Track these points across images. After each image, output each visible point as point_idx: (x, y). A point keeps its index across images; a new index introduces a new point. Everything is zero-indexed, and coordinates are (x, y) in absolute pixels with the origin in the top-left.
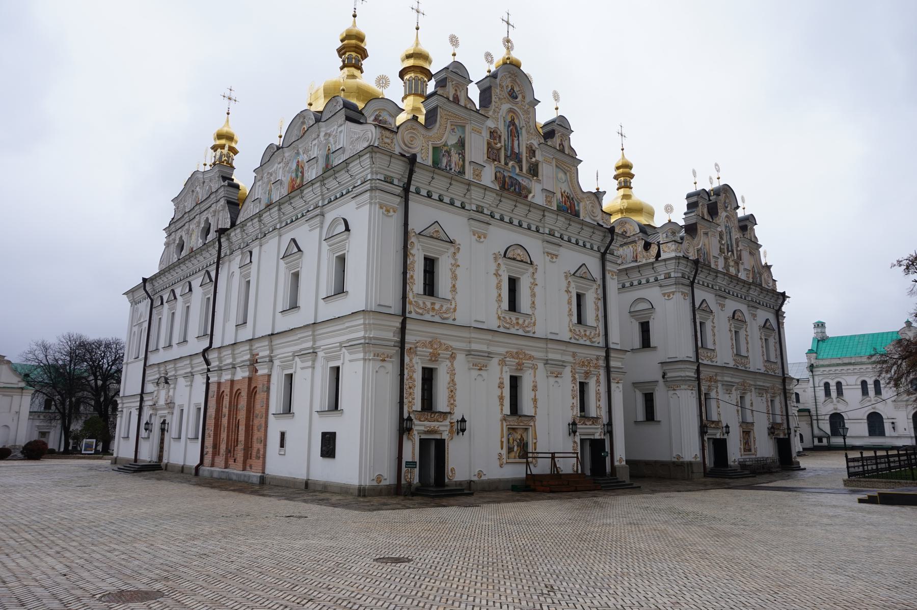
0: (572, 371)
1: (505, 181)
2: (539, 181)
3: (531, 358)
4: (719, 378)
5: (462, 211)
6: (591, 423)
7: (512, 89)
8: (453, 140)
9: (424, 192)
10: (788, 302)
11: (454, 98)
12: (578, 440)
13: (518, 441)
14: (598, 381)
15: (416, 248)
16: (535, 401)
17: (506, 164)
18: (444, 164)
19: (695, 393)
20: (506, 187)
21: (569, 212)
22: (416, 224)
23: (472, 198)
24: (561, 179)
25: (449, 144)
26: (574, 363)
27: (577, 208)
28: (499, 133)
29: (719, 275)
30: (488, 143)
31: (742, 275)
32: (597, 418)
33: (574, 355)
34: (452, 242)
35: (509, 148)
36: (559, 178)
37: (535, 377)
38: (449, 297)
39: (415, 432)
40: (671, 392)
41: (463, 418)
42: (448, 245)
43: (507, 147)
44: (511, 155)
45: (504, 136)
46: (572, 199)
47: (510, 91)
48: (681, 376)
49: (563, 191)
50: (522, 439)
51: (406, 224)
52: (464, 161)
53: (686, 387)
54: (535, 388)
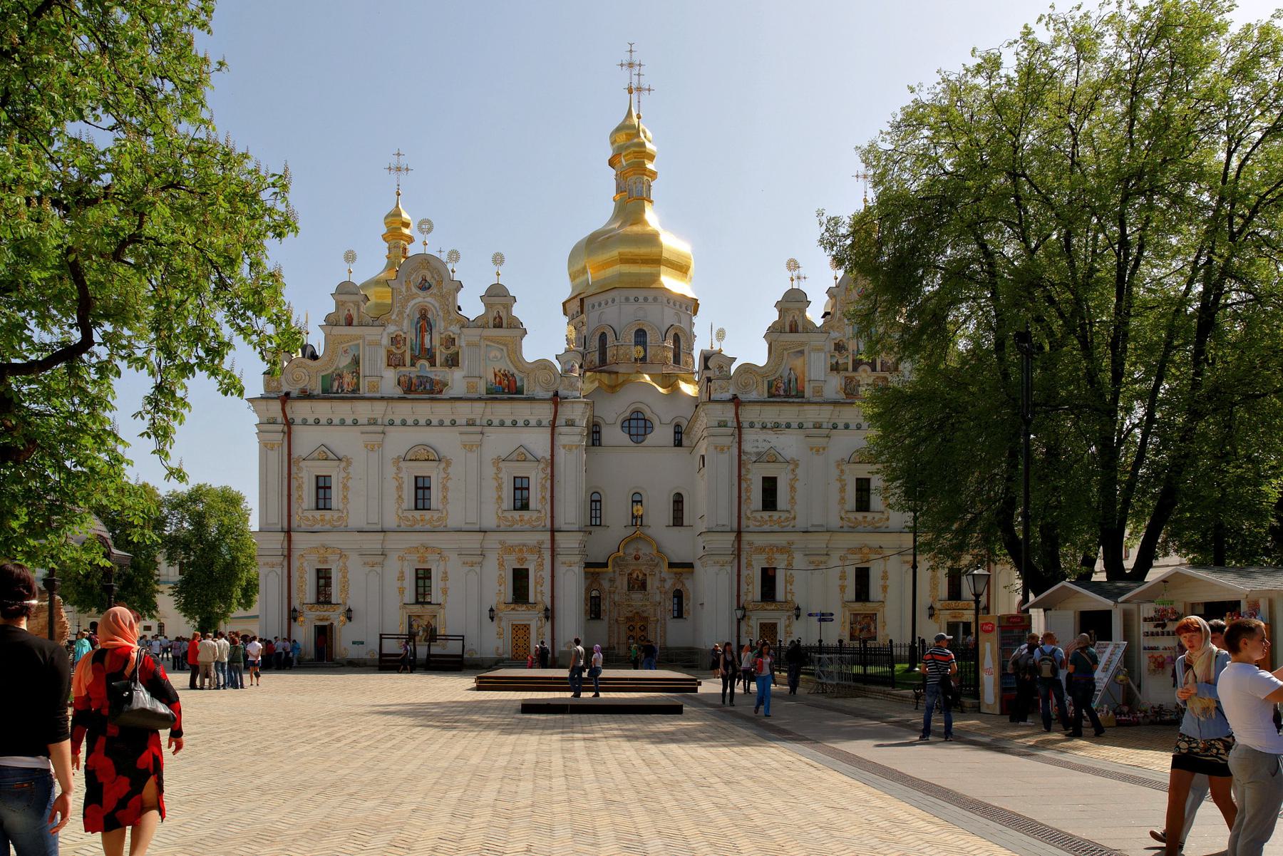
5: (355, 428)
6: (524, 607)
7: (424, 280)
8: (345, 361)
11: (346, 319)
12: (506, 626)
16: (445, 592)
18: (335, 389)
19: (730, 570)
22: (301, 449)
24: (496, 357)
27: (519, 384)
28: (403, 336)
30: (390, 354)
33: (502, 543)
38: (341, 508)
45: (411, 336)
46: (513, 375)
50: (429, 625)
52: (358, 378)
54: (445, 578)
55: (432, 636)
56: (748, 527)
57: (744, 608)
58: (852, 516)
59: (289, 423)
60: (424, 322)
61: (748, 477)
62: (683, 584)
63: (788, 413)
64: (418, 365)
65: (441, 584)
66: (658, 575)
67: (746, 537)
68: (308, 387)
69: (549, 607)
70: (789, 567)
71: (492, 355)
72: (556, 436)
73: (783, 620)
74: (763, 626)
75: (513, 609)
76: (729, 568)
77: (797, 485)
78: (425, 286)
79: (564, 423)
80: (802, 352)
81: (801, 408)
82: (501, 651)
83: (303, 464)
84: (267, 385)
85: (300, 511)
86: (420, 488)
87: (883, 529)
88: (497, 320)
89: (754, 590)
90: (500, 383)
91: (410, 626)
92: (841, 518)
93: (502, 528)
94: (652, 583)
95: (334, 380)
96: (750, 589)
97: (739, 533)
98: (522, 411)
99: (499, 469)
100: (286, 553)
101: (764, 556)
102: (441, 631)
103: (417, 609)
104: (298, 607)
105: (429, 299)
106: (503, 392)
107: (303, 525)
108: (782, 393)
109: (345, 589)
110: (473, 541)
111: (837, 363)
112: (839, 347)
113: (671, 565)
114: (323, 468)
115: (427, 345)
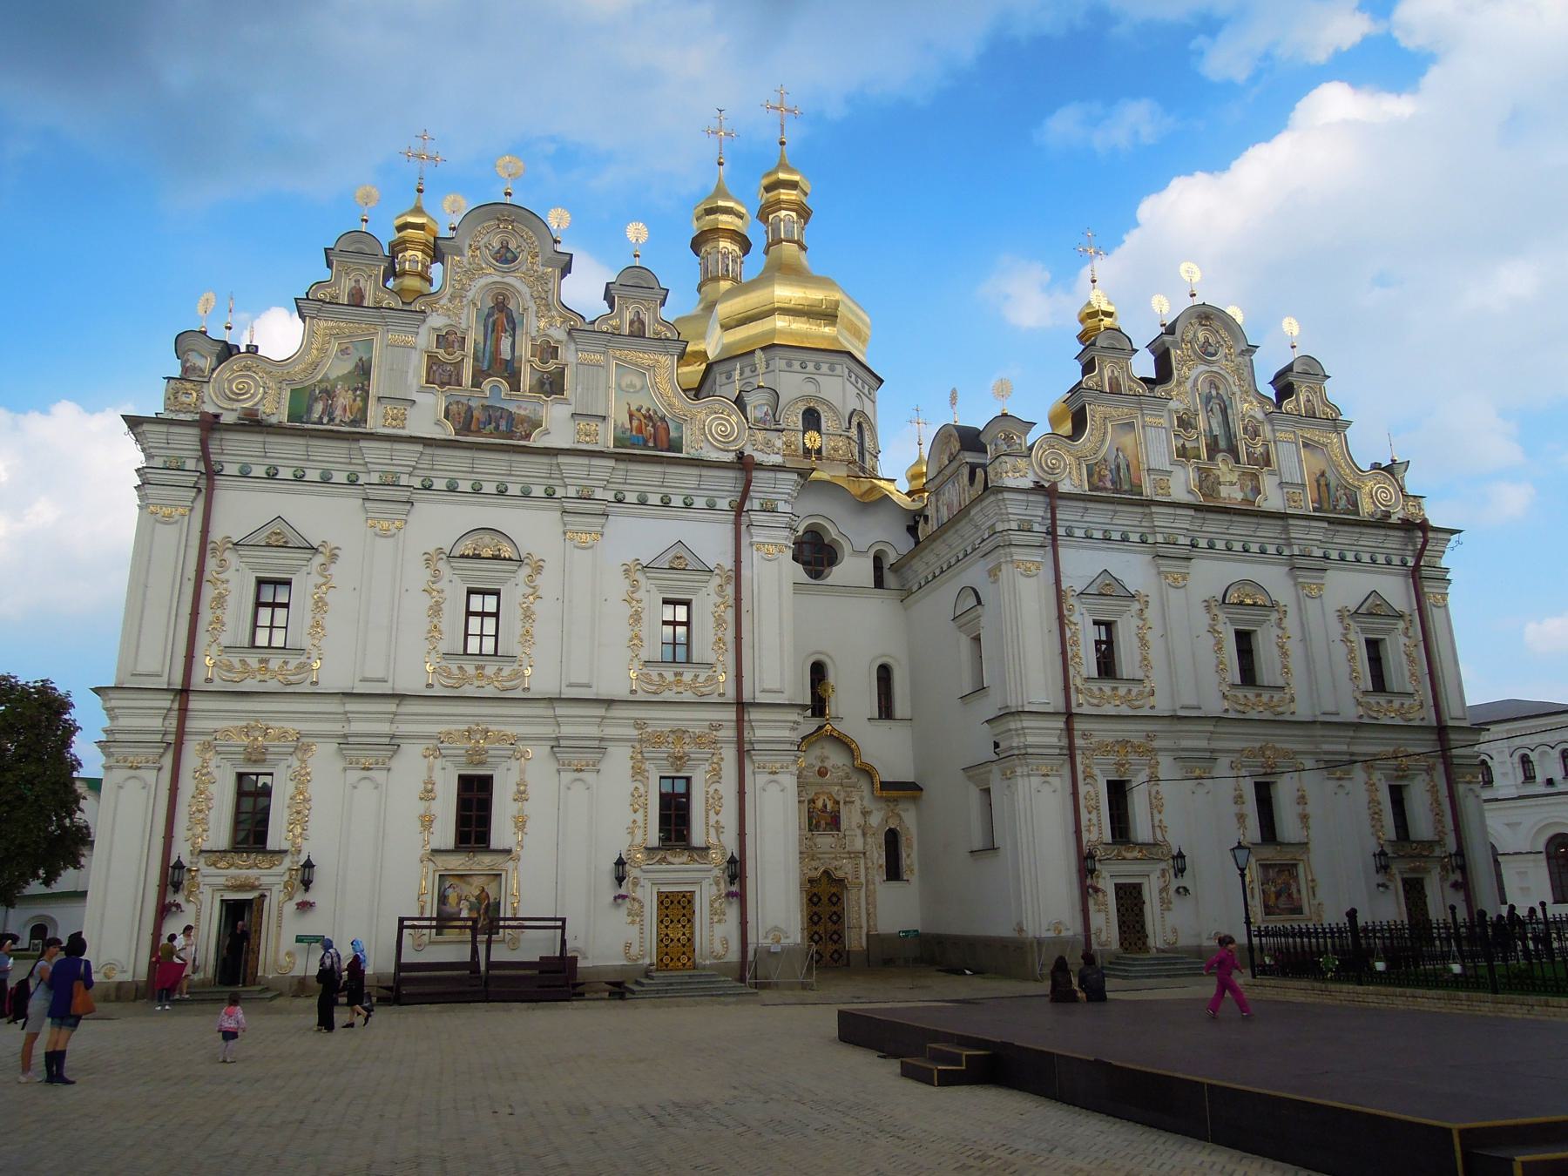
0: (632, 758)
1: (472, 417)
2: (566, 402)
3: (502, 738)
4: (1156, 744)
5: (352, 490)
6: (685, 858)
8: (346, 366)
9: (259, 471)
10: (1458, 542)
11: (351, 295)
12: (648, 897)
13: (473, 899)
14: (717, 774)
15: (233, 568)
16: (520, 824)
17: (476, 384)
18: (316, 416)
19: (1060, 783)
20: (473, 427)
21: (651, 444)
23: (366, 463)
24: (632, 385)
25: (331, 378)
26: (641, 741)
27: (673, 434)
29: (1154, 509)
30: (432, 359)
31: (1272, 499)
32: (708, 848)
33: (639, 724)
34: (314, 548)
35: (487, 355)
36: (624, 384)
37: (522, 771)
39: (207, 891)
40: (1006, 783)
41: (309, 859)
42: (306, 555)
43: (480, 354)
44: (489, 369)
45: (474, 337)
46: (663, 419)
47: (498, 252)
48: (1018, 748)
49: (633, 408)
51: (205, 531)
52: (365, 399)
53: (1025, 769)
54: (521, 796)
55: (488, 919)
56: (1080, 705)
57: (1091, 856)
58: (1240, 693)
59: (212, 471)
60: (501, 316)
61: (1071, 619)
62: (901, 819)
63: (1126, 520)
64: (487, 385)
65: (513, 807)
66: (858, 803)
67: (1079, 726)
68: (261, 408)
69: (738, 859)
70: (1154, 779)
71: (626, 381)
72: (743, 527)
73: (1153, 877)
74: (1118, 887)
75: (663, 860)
76: (1056, 781)
77: (1150, 636)
78: (505, 257)
79: (756, 506)
80: (1131, 426)
81: (1147, 510)
82: (634, 950)
83: (227, 555)
84: (172, 398)
85: (215, 649)
86: (476, 614)
87: (1287, 717)
88: (636, 323)
89: (1099, 828)
90: (640, 430)
91: (443, 899)
92: (1225, 697)
93: (641, 696)
94: (851, 818)
95: (317, 400)
96: (1095, 821)
97: (1069, 716)
98: (682, 481)
99: (635, 586)
100: (171, 738)
101: (1113, 758)
102: (506, 911)
103: (458, 863)
104: (186, 861)
105: (509, 280)
106: (646, 447)
107: (217, 680)
108: (1109, 485)
109: (300, 816)
110: (578, 725)
111: (1183, 445)
112: (1185, 423)
113: (885, 786)
114: (275, 560)
115: (506, 353)
